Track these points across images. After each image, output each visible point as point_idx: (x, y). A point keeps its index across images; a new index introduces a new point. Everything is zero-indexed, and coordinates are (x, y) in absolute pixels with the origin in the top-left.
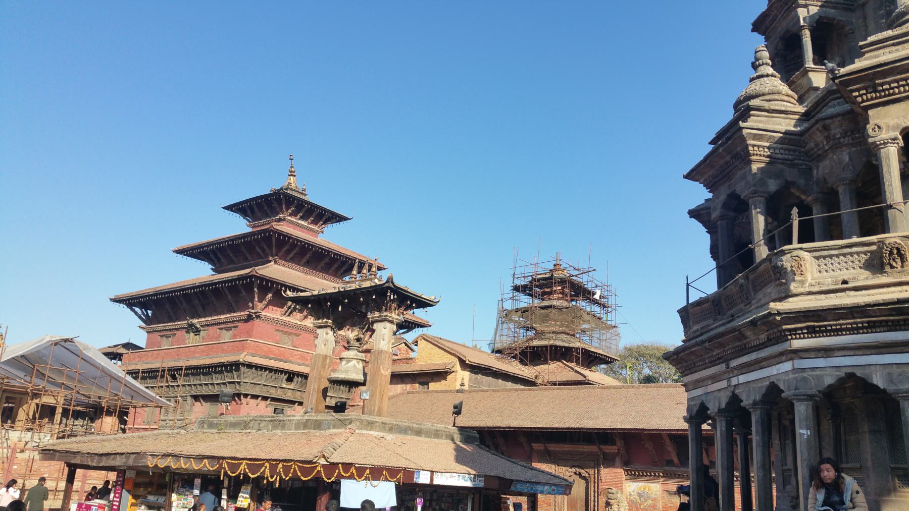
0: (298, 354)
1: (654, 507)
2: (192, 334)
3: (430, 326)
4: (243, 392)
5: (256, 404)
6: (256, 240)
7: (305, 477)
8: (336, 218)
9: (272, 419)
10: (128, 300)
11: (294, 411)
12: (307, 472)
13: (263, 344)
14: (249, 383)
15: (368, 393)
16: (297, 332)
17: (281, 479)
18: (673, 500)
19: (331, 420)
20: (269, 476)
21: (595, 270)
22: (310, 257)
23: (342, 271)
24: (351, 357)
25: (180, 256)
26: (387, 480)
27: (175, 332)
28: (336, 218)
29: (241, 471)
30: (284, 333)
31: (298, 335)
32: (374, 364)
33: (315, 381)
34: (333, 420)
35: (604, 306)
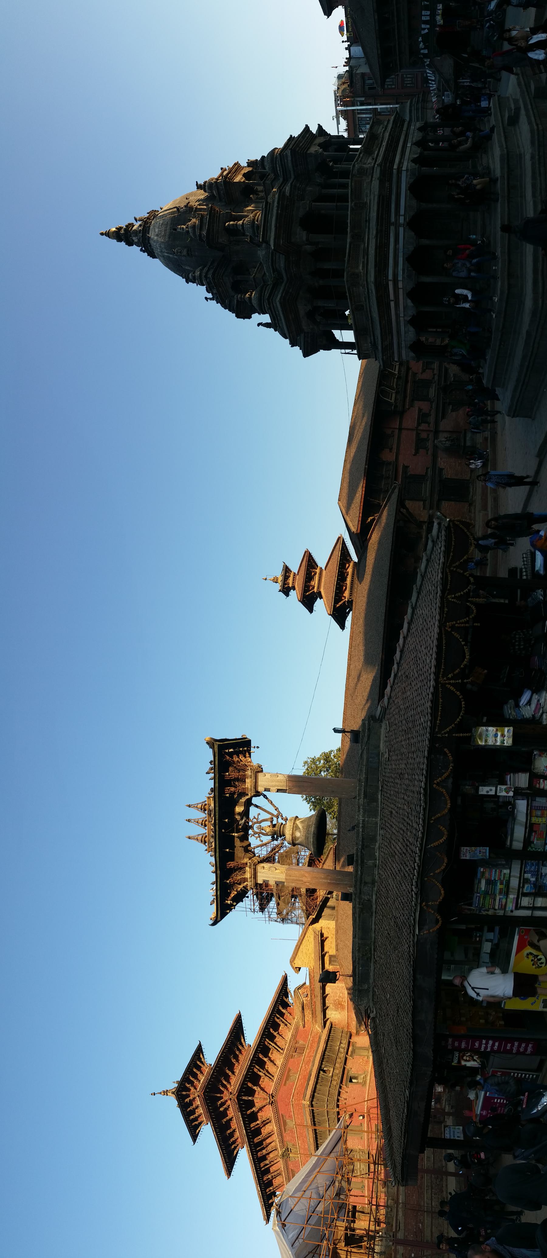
4: (336, 1102)
14: (328, 1098)
30: (287, 1079)
31: (289, 1070)
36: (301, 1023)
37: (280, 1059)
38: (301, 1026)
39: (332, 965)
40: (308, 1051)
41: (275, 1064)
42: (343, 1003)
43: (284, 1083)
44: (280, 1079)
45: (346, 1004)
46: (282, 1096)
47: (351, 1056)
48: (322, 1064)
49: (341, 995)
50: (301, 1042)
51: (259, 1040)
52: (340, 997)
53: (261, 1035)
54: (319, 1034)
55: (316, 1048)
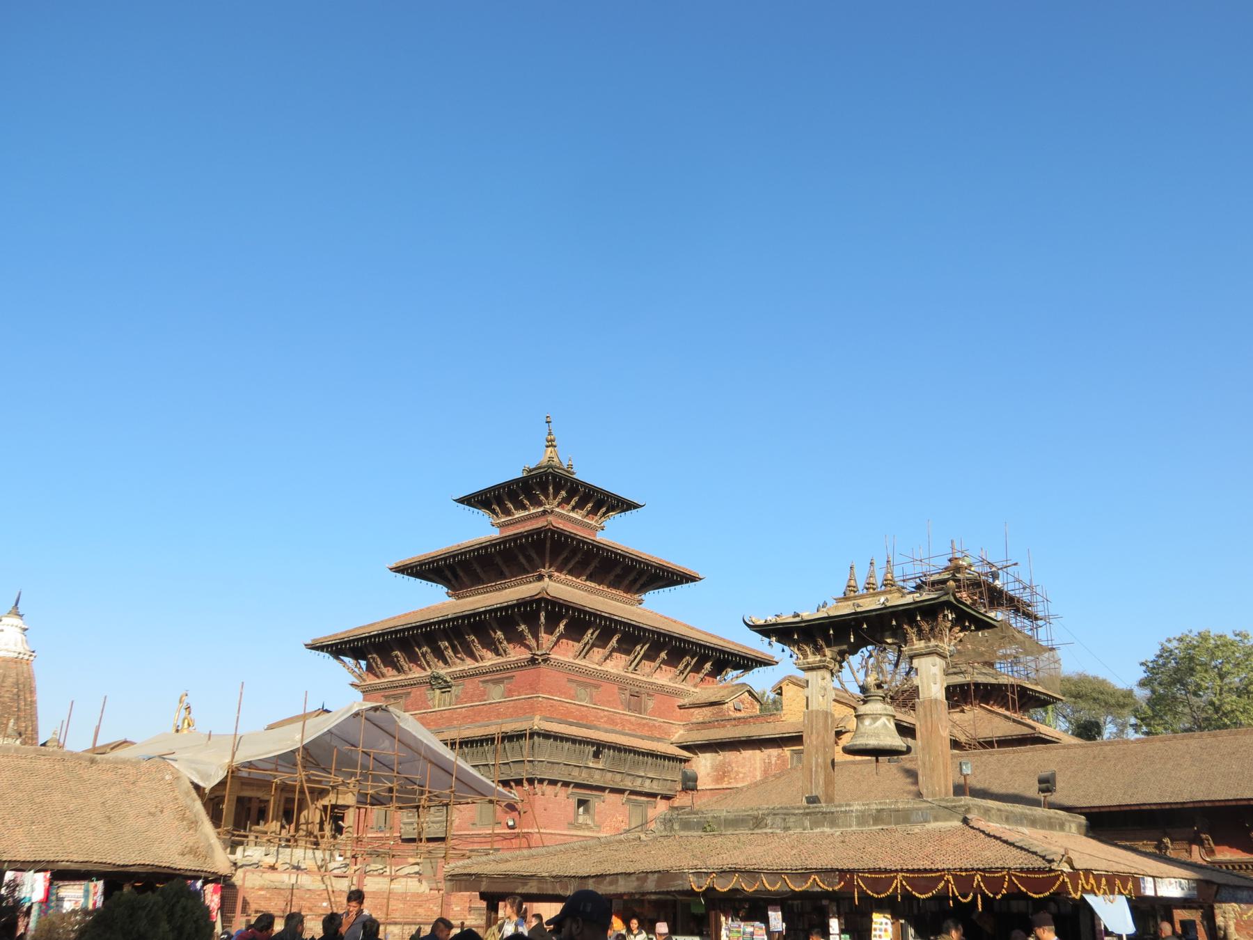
0: (605, 716)
2: (438, 691)
3: (777, 663)
4: (539, 777)
5: (553, 794)
6: (522, 548)
7: (921, 894)
8: (625, 505)
9: (807, 811)
10: (336, 644)
11: (603, 802)
12: (1039, 885)
14: (546, 762)
15: (969, 765)
16: (596, 682)
17: (984, 896)
19: (927, 808)
20: (957, 894)
21: (1016, 564)
22: (596, 567)
23: (638, 585)
24: (880, 712)
25: (399, 576)
26: (1120, 893)
27: (409, 690)
28: (625, 505)
29: (897, 887)
30: (580, 684)
31: (597, 687)
32: (926, 722)
33: (816, 753)
34: (932, 808)
35: (1036, 619)
37: (616, 666)
38: (681, 702)
39: (792, 756)
40: (633, 719)
41: (605, 660)
42: (726, 779)
45: (725, 786)
46: (547, 676)
47: (628, 800)
49: (741, 775)
50: (651, 704)
51: (648, 627)
52: (738, 773)
53: (658, 630)
55: (639, 734)
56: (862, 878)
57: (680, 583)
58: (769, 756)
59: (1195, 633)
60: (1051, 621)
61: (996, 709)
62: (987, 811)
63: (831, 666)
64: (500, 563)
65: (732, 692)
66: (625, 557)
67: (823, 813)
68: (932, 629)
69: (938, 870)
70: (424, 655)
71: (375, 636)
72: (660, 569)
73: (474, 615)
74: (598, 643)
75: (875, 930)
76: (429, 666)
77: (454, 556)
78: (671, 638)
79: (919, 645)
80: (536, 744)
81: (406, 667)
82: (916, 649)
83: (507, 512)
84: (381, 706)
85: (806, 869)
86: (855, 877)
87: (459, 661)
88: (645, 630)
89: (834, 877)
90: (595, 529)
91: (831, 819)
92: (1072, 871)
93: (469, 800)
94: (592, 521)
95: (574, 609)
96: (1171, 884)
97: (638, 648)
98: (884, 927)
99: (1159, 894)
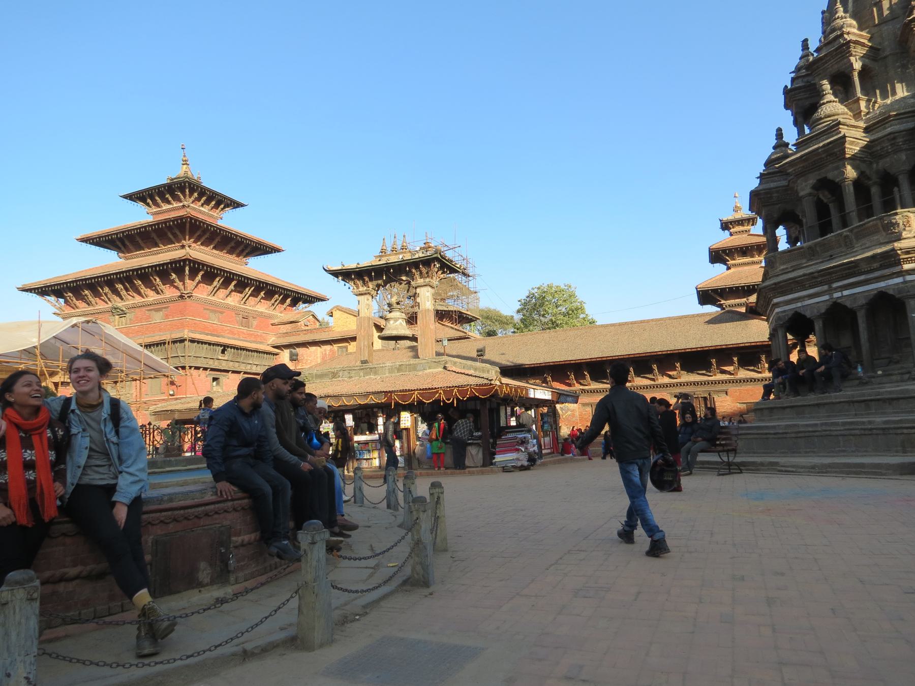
0: (228, 330)
1: (573, 415)
2: (117, 317)
5: (197, 375)
6: (170, 228)
8: (236, 205)
10: (41, 288)
12: (484, 392)
13: (199, 322)
18: (586, 409)
19: (425, 363)
21: (460, 246)
22: (218, 241)
23: (245, 254)
24: (398, 317)
25: (84, 244)
28: (236, 205)
29: (414, 398)
31: (222, 313)
32: (423, 321)
33: (364, 339)
34: (428, 363)
35: (469, 276)
36: (276, 321)
37: (233, 301)
38: (273, 322)
39: (338, 350)
40: (245, 331)
41: (227, 297)
42: (300, 364)
43: (208, 307)
44: (212, 303)
48: (231, 348)
49: (309, 361)
50: (255, 323)
52: (307, 360)
53: (259, 280)
54: (265, 341)
56: (396, 395)
57: (271, 253)
58: (325, 350)
59: (546, 285)
60: (476, 277)
61: (446, 323)
62: (455, 363)
63: (372, 293)
64: (155, 238)
65: (303, 315)
66: (237, 236)
67: (370, 368)
68: (427, 273)
69: (435, 388)
70: (106, 294)
71: (70, 282)
72: (259, 244)
73: (141, 269)
74: (221, 287)
75: (402, 421)
76: (110, 301)
77: (123, 232)
78: (267, 284)
79: (420, 281)
80: (187, 346)
81: (93, 302)
82: (418, 283)
83: (158, 205)
84: (91, 320)
85: (367, 392)
86: (393, 395)
87: (131, 298)
88: (251, 279)
89: (382, 396)
90: (217, 218)
91: (374, 371)
92: (500, 384)
93: (152, 376)
94: (215, 213)
95: (208, 266)
96: (541, 393)
97: (247, 289)
98: (406, 419)
99: (536, 397)
